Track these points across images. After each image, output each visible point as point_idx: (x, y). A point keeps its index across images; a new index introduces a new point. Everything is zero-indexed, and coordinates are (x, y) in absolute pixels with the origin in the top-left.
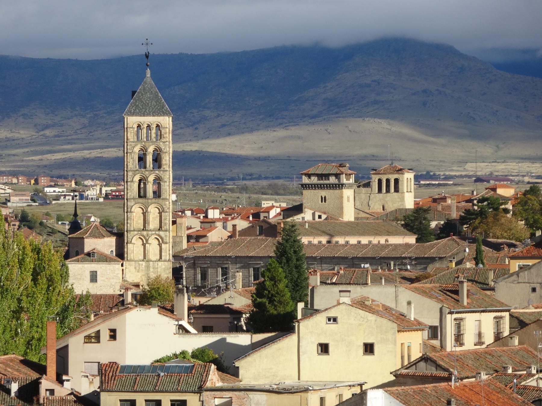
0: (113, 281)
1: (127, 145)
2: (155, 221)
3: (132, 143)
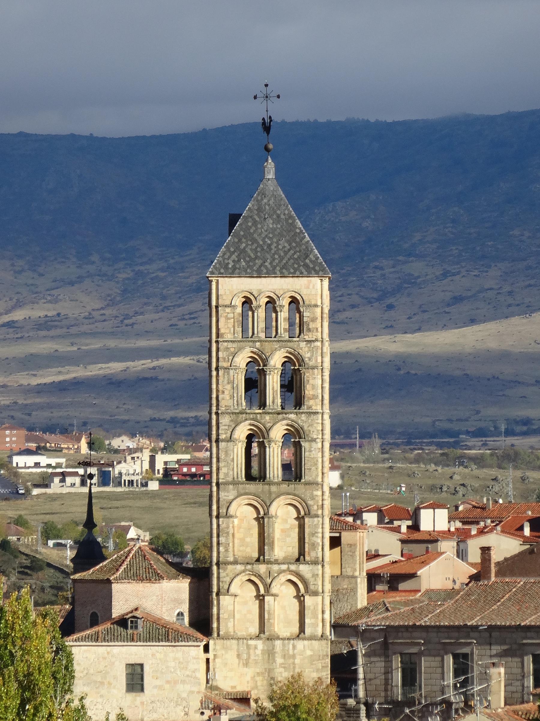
0: (183, 689)
1: (218, 350)
2: (288, 540)
3: (230, 345)
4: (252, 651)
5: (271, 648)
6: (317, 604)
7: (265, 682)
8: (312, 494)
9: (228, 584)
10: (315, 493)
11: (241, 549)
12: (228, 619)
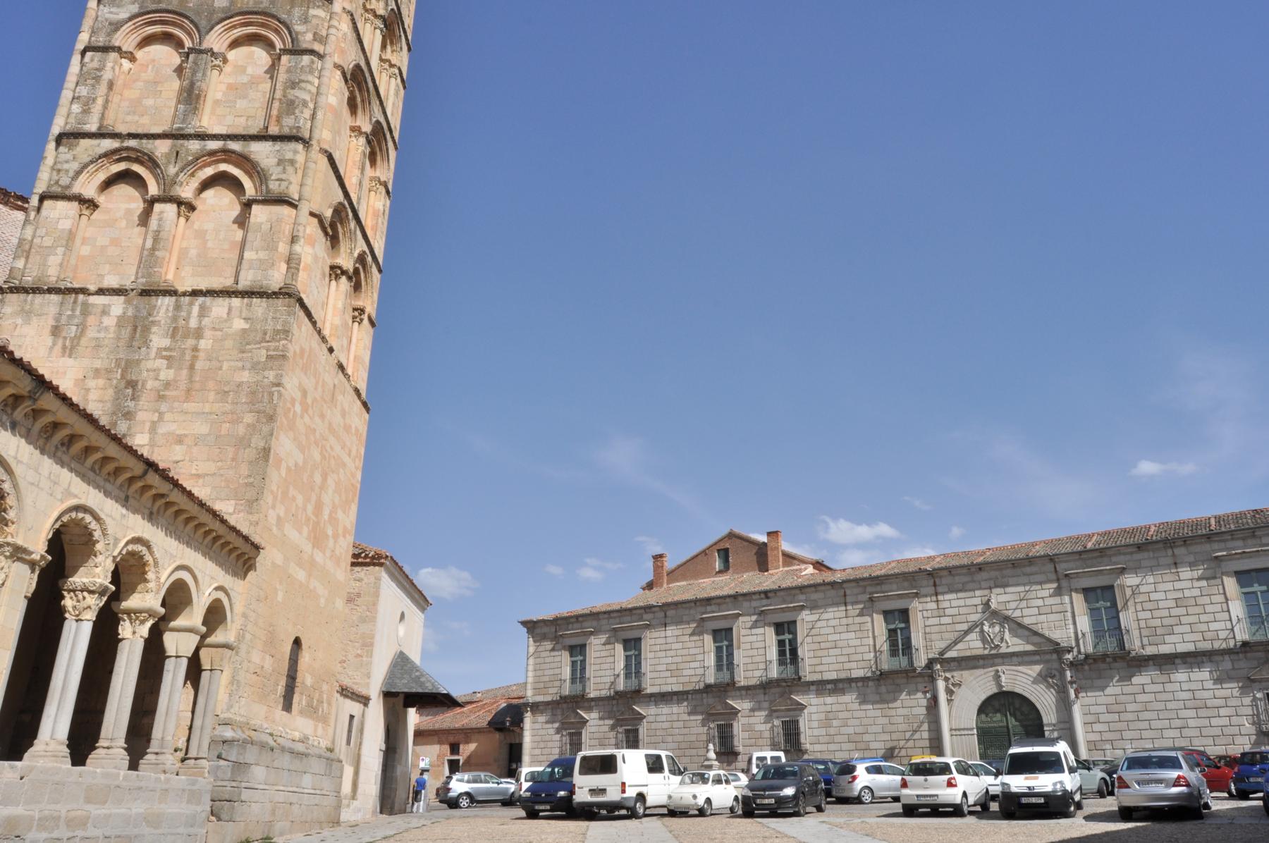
4: (91, 320)
6: (279, 220)
7: (111, 392)
8: (306, 13)
9: (71, 174)
10: (312, 12)
11: (129, 118)
12: (51, 249)
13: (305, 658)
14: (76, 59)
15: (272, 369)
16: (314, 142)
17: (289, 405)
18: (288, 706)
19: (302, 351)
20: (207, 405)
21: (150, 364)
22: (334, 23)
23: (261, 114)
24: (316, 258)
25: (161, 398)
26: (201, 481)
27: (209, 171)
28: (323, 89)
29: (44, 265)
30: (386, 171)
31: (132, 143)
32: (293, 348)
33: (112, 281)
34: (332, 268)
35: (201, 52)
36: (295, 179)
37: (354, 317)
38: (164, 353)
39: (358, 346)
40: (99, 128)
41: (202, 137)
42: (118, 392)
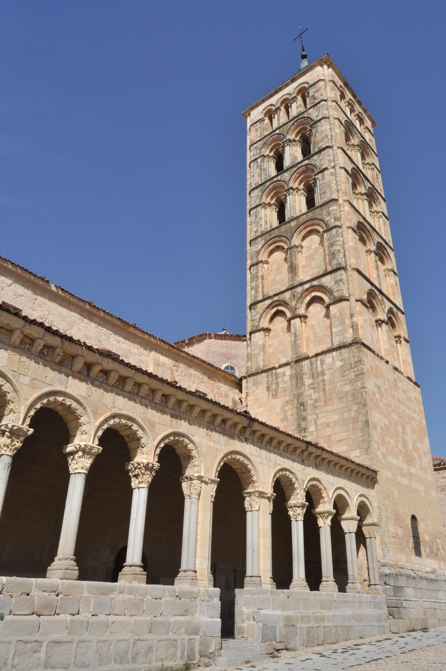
3: (258, 144)
4: (280, 380)
5: (299, 371)
7: (295, 410)
9: (258, 320)
10: (331, 209)
11: (273, 288)
13: (421, 526)
14: (248, 272)
15: (359, 381)
16: (348, 267)
17: (372, 396)
18: (418, 553)
19: (371, 367)
20: (335, 406)
21: (307, 393)
22: (342, 209)
23: (323, 263)
24: (365, 321)
25: (315, 407)
26: (342, 443)
27: (308, 298)
28: (345, 241)
29: (257, 362)
30: (391, 263)
31: (276, 298)
32: (366, 368)
33: (283, 361)
34: (376, 321)
35: (291, 248)
36: (344, 287)
37: (396, 341)
38: (311, 386)
39: (403, 356)
40: (263, 297)
41: (301, 284)
42: (298, 409)
